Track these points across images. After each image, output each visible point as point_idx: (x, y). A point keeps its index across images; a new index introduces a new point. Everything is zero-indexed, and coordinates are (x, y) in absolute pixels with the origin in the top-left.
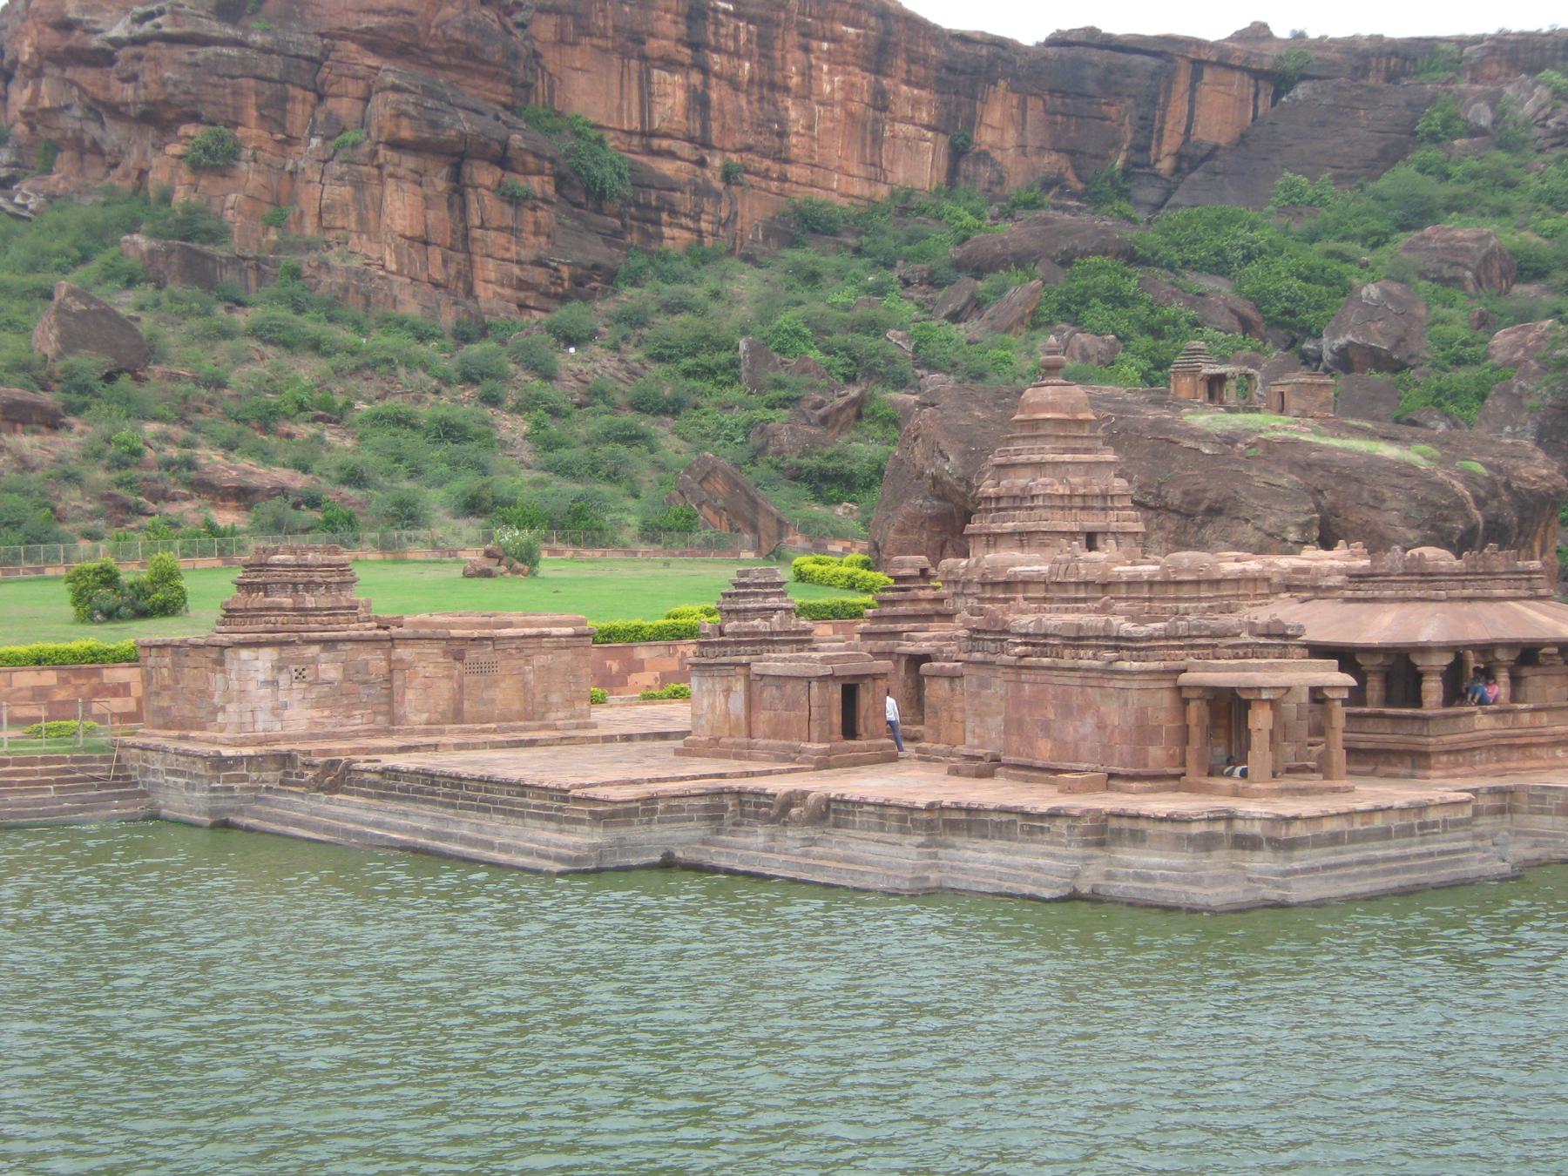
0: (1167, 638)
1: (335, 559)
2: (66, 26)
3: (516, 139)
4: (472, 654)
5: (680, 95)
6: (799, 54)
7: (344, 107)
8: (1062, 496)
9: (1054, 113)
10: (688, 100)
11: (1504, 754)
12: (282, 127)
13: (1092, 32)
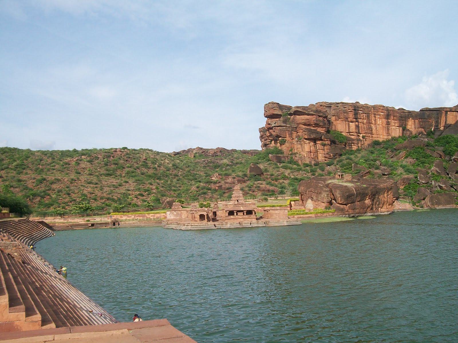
2: (269, 124)
6: (374, 118)
10: (355, 127)
13: (427, 108)
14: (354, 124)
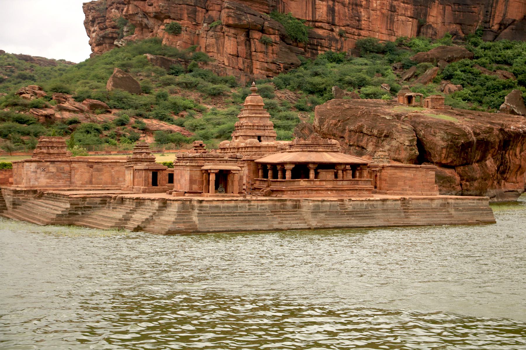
0: (200, 158)
1: (61, 140)
3: (266, 24)
4: (95, 166)
5: (325, 8)
7: (213, 14)
8: (250, 126)
9: (455, 11)
11: (310, 192)
12: (195, 20)
14: (324, 3)
